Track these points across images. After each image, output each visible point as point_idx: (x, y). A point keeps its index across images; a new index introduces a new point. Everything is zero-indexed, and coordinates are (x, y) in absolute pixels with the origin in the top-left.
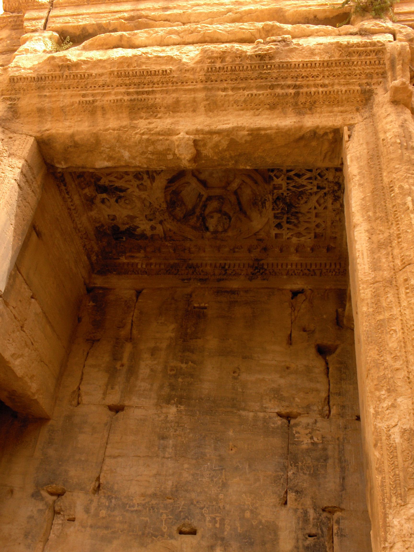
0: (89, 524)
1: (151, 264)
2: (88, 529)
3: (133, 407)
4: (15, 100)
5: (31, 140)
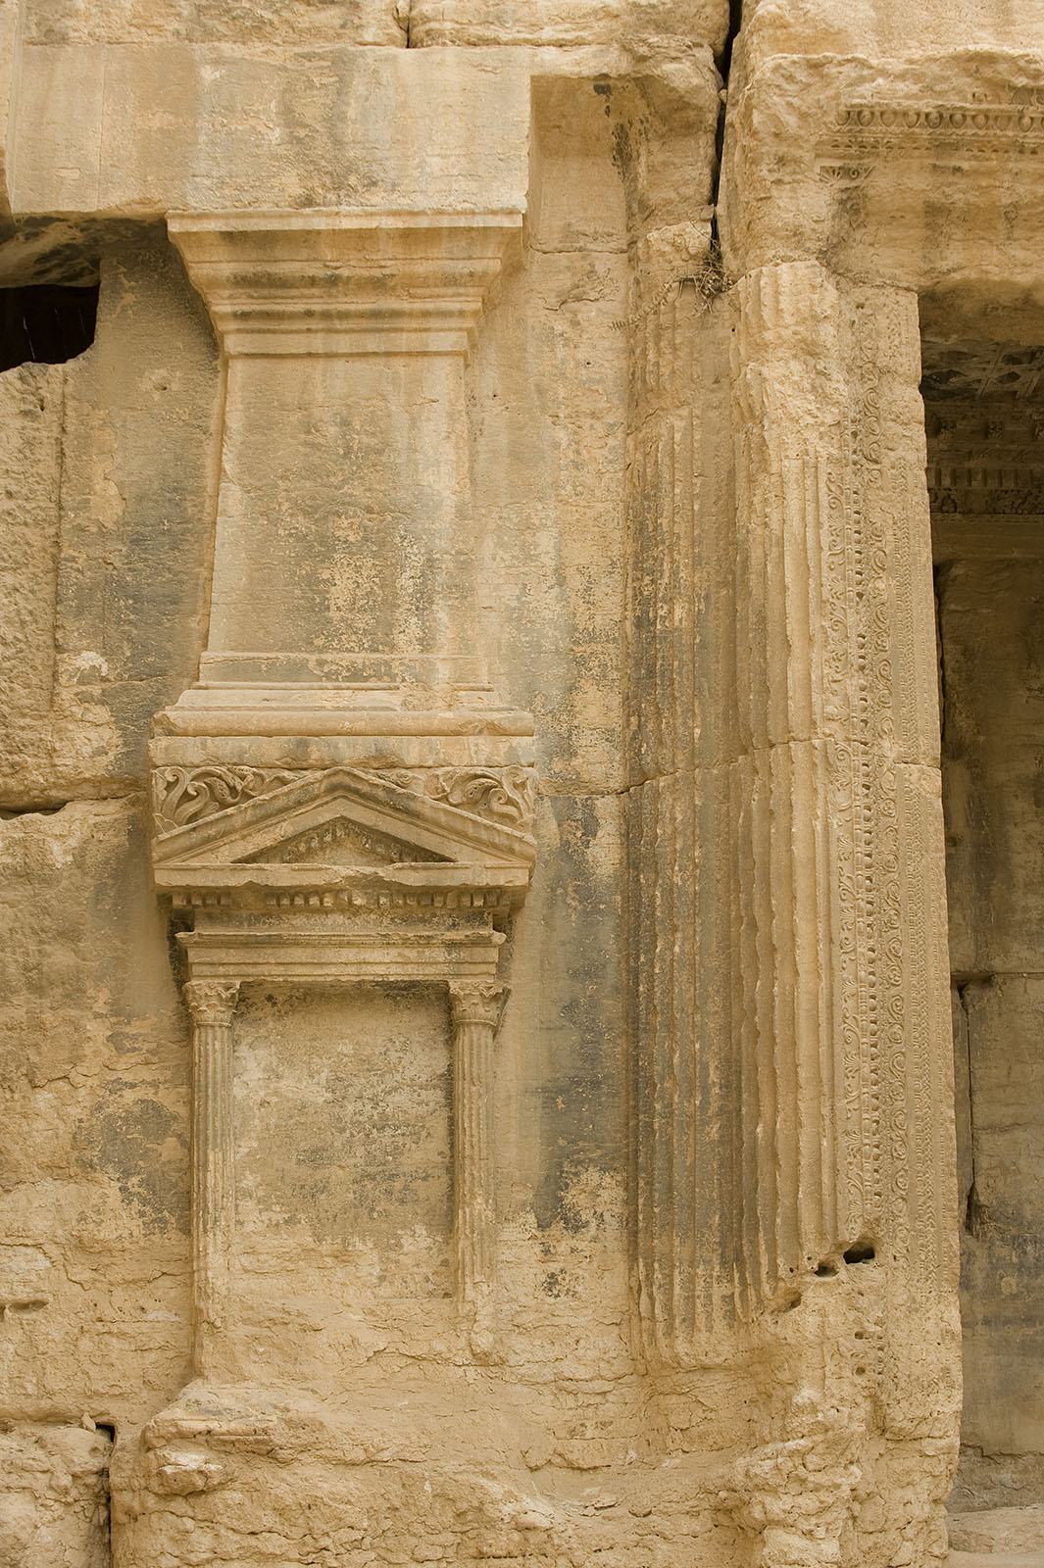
0: (980, 1317)
1: (970, 475)
2: (980, 1328)
3: (1020, 975)
4: (857, 173)
5: (910, 306)
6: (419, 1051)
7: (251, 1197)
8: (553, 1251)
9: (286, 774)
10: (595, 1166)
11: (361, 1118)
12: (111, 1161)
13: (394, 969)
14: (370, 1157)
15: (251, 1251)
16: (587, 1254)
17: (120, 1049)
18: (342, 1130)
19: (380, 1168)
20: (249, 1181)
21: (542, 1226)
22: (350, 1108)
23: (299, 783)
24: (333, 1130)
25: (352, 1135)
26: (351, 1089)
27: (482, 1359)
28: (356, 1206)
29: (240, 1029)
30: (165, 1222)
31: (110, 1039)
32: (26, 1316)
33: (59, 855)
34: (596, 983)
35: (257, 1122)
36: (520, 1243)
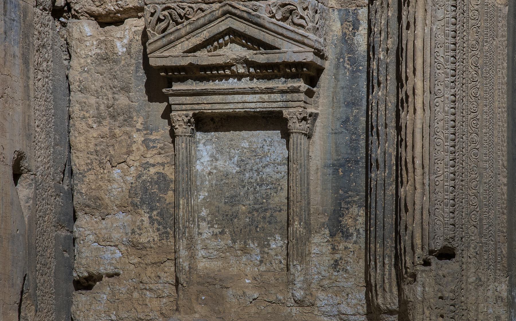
6: (277, 145)
7: (205, 221)
8: (337, 248)
9: (204, 6)
10: (356, 205)
11: (252, 181)
12: (145, 204)
13: (259, 105)
14: (256, 200)
15: (206, 248)
16: (352, 250)
17: (148, 148)
18: (244, 187)
19: (260, 206)
20: (204, 213)
21: (332, 235)
22: (247, 175)
23: (209, 11)
24: (240, 187)
25: (248, 189)
26: (247, 166)
27: (299, 303)
28: (250, 225)
29: (199, 135)
30: (169, 234)
31: (143, 142)
32: (111, 280)
33: (120, 49)
34: (358, 109)
35: (207, 183)
36: (322, 244)
